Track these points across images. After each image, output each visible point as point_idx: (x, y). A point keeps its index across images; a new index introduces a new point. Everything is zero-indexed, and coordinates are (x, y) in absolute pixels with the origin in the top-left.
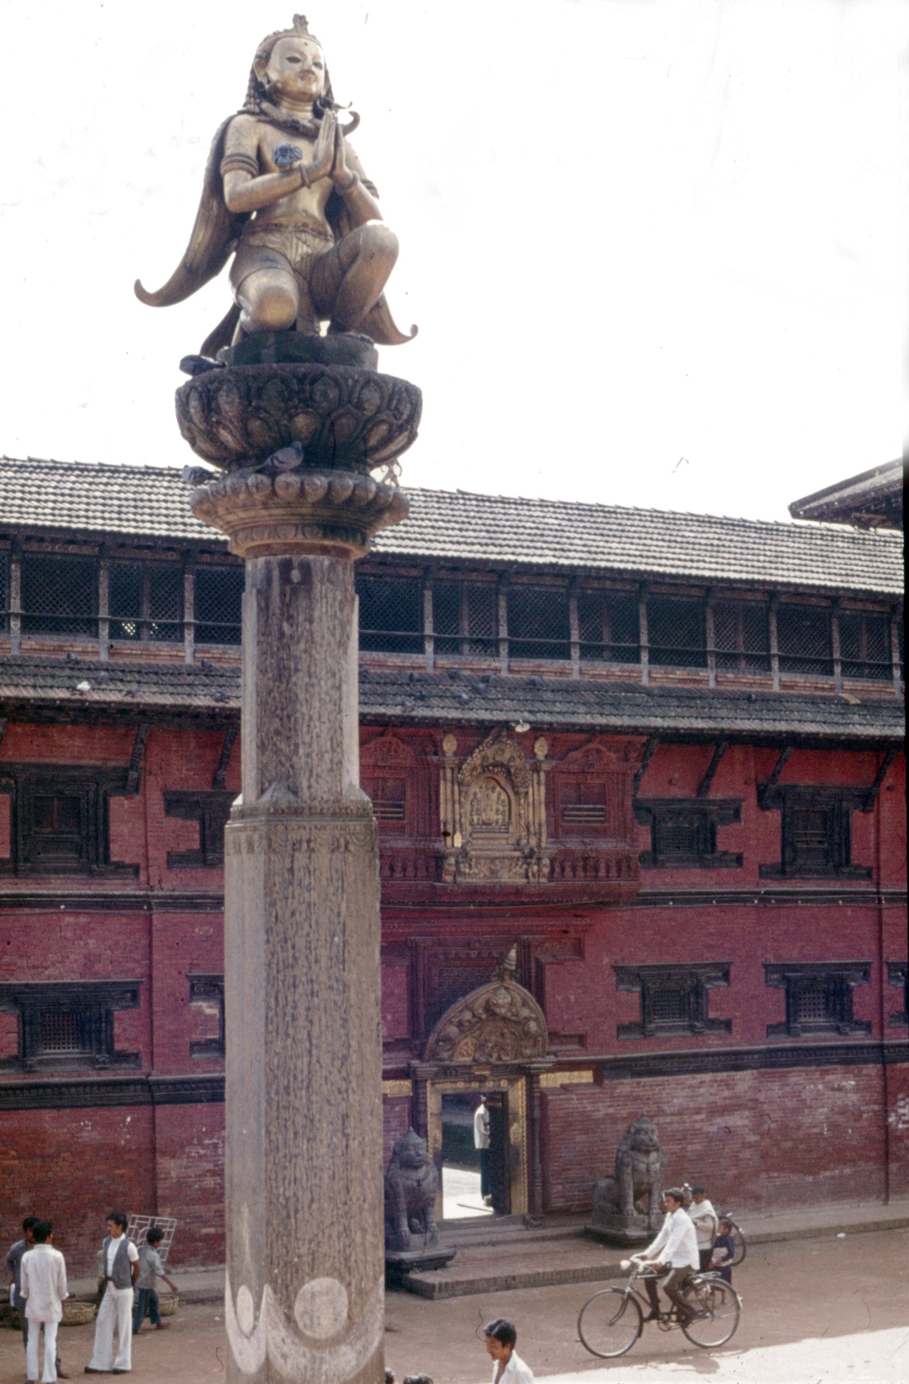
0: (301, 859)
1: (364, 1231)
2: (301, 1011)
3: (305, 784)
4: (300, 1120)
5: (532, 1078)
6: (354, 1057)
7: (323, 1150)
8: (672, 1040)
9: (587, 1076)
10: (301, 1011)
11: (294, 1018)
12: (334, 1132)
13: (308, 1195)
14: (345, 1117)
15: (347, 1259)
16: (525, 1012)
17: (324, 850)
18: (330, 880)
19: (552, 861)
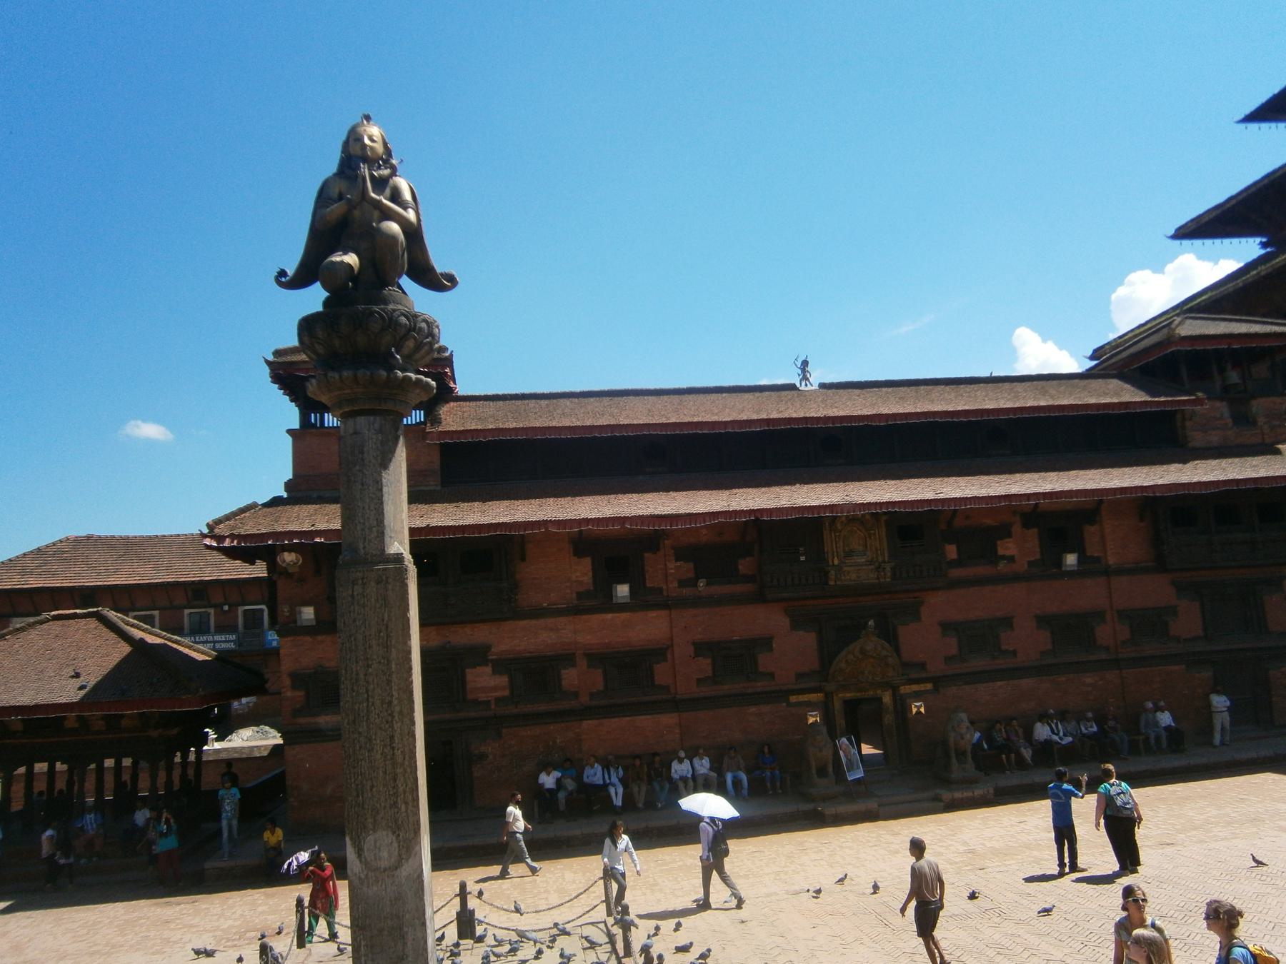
0: (358, 589)
1: (406, 803)
2: (362, 676)
3: (361, 546)
4: (362, 739)
5: (895, 689)
6: (395, 702)
7: (378, 756)
8: (979, 663)
9: (929, 686)
10: (362, 676)
11: (357, 680)
12: (385, 746)
13: (369, 783)
14: (392, 737)
15: (396, 821)
16: (884, 653)
17: (373, 584)
18: (377, 600)
19: (893, 569)
